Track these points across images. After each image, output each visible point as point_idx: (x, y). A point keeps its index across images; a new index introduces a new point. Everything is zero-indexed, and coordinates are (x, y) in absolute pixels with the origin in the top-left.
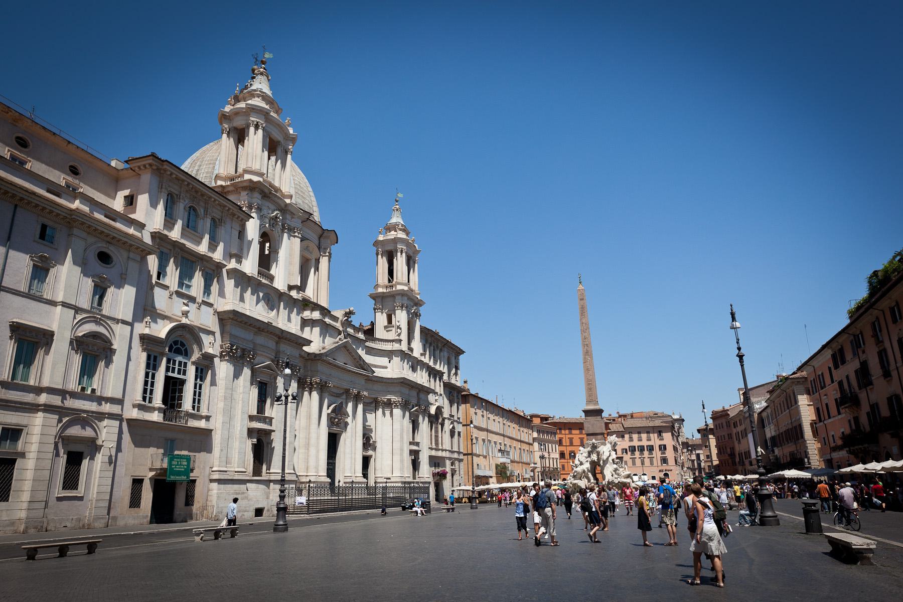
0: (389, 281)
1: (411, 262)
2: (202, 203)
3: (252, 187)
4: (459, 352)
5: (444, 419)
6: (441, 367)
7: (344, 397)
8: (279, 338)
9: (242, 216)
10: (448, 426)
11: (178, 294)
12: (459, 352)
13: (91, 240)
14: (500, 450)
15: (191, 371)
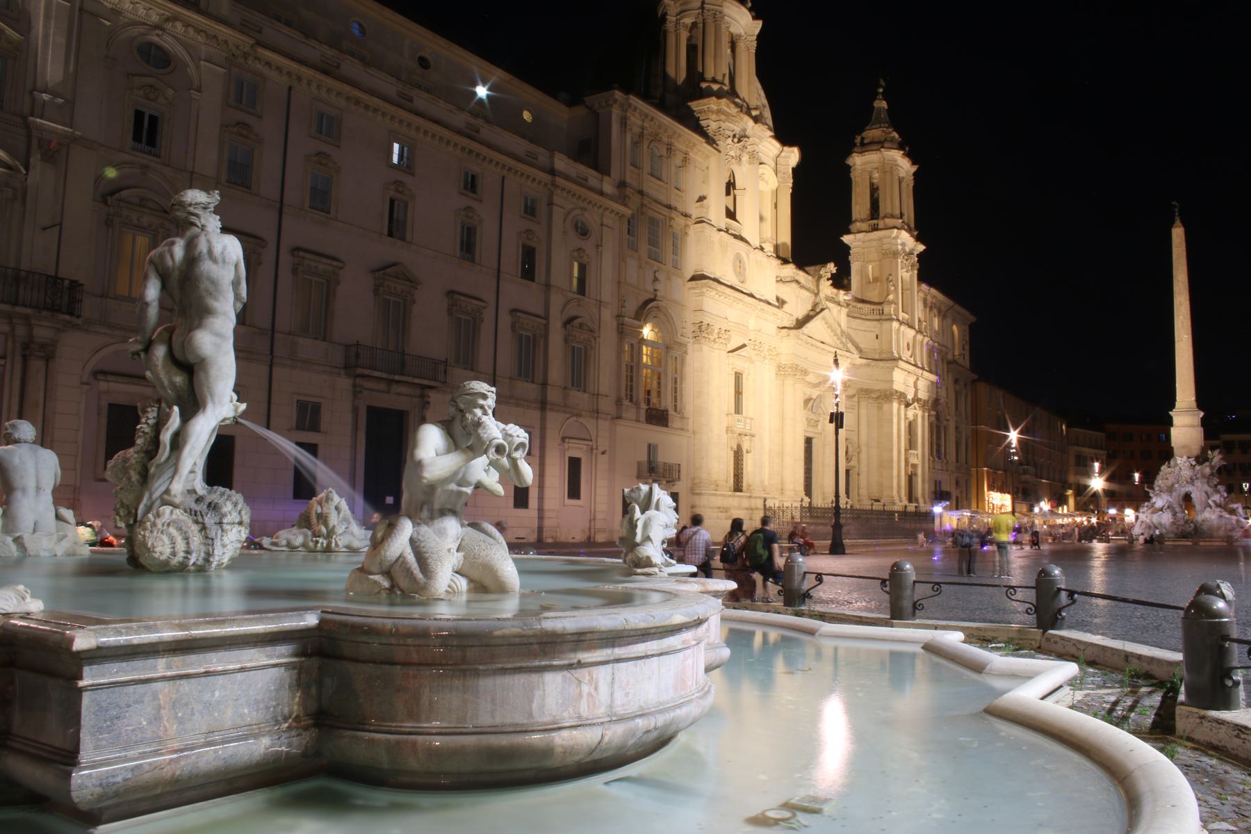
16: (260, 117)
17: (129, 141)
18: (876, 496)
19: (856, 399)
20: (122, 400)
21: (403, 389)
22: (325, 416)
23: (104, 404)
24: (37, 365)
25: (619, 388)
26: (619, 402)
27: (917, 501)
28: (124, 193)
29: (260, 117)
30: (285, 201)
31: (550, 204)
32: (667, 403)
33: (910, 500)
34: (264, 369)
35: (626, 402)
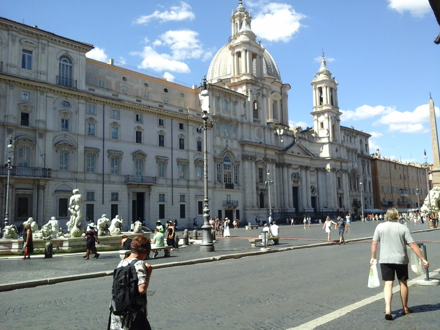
0: (321, 104)
1: (333, 91)
2: (228, 97)
3: (247, 82)
4: (368, 136)
5: (358, 176)
6: (358, 146)
7: (299, 169)
8: (266, 148)
9: (244, 97)
10: (361, 179)
11: (224, 137)
12: (368, 136)
13: (194, 125)
14: (400, 190)
15: (233, 168)
16: (96, 115)
17: (61, 128)
18: (326, 206)
19: (316, 171)
20: (63, 197)
21: (143, 186)
22: (120, 197)
23: (58, 198)
24: (41, 191)
25: (215, 178)
26: (215, 183)
27: (344, 207)
28: (60, 143)
29: (96, 115)
30: (105, 137)
31: (188, 125)
32: (233, 181)
33: (341, 206)
34: (102, 185)
35: (218, 183)
